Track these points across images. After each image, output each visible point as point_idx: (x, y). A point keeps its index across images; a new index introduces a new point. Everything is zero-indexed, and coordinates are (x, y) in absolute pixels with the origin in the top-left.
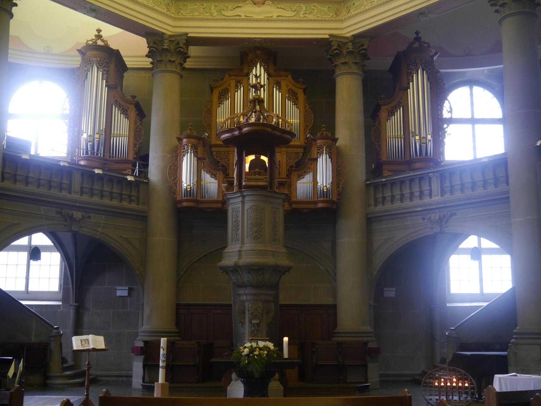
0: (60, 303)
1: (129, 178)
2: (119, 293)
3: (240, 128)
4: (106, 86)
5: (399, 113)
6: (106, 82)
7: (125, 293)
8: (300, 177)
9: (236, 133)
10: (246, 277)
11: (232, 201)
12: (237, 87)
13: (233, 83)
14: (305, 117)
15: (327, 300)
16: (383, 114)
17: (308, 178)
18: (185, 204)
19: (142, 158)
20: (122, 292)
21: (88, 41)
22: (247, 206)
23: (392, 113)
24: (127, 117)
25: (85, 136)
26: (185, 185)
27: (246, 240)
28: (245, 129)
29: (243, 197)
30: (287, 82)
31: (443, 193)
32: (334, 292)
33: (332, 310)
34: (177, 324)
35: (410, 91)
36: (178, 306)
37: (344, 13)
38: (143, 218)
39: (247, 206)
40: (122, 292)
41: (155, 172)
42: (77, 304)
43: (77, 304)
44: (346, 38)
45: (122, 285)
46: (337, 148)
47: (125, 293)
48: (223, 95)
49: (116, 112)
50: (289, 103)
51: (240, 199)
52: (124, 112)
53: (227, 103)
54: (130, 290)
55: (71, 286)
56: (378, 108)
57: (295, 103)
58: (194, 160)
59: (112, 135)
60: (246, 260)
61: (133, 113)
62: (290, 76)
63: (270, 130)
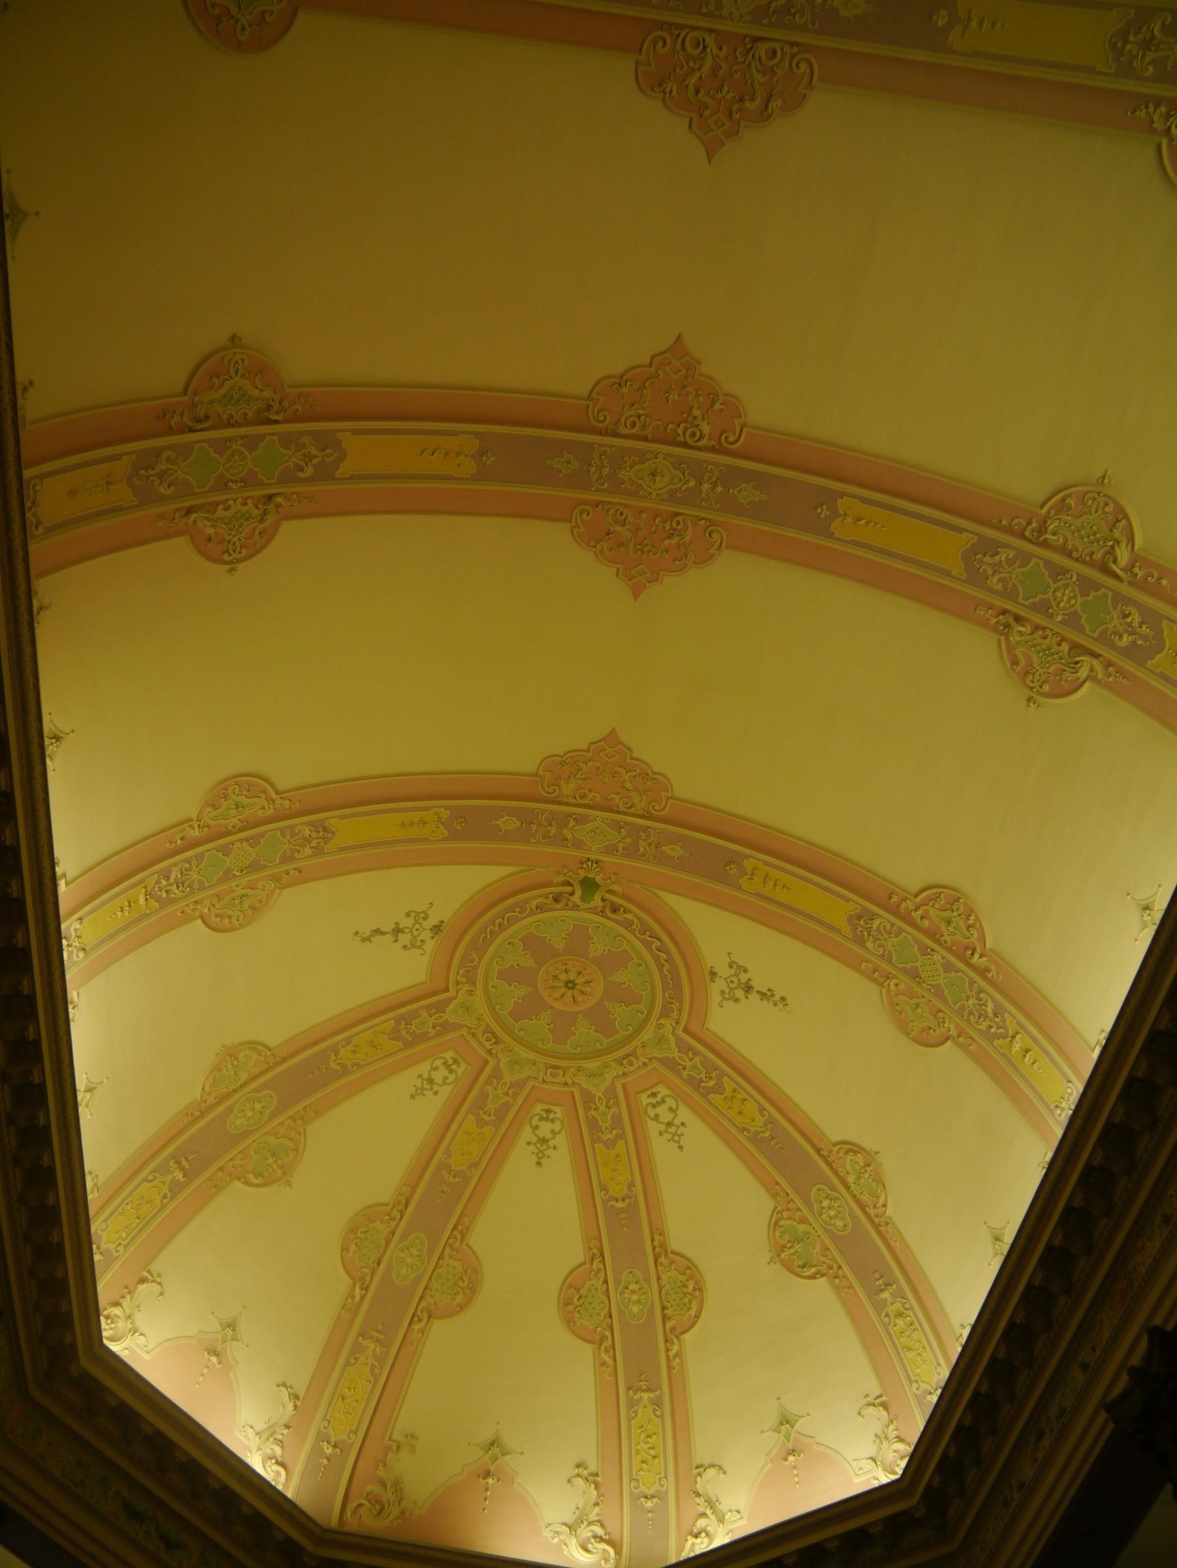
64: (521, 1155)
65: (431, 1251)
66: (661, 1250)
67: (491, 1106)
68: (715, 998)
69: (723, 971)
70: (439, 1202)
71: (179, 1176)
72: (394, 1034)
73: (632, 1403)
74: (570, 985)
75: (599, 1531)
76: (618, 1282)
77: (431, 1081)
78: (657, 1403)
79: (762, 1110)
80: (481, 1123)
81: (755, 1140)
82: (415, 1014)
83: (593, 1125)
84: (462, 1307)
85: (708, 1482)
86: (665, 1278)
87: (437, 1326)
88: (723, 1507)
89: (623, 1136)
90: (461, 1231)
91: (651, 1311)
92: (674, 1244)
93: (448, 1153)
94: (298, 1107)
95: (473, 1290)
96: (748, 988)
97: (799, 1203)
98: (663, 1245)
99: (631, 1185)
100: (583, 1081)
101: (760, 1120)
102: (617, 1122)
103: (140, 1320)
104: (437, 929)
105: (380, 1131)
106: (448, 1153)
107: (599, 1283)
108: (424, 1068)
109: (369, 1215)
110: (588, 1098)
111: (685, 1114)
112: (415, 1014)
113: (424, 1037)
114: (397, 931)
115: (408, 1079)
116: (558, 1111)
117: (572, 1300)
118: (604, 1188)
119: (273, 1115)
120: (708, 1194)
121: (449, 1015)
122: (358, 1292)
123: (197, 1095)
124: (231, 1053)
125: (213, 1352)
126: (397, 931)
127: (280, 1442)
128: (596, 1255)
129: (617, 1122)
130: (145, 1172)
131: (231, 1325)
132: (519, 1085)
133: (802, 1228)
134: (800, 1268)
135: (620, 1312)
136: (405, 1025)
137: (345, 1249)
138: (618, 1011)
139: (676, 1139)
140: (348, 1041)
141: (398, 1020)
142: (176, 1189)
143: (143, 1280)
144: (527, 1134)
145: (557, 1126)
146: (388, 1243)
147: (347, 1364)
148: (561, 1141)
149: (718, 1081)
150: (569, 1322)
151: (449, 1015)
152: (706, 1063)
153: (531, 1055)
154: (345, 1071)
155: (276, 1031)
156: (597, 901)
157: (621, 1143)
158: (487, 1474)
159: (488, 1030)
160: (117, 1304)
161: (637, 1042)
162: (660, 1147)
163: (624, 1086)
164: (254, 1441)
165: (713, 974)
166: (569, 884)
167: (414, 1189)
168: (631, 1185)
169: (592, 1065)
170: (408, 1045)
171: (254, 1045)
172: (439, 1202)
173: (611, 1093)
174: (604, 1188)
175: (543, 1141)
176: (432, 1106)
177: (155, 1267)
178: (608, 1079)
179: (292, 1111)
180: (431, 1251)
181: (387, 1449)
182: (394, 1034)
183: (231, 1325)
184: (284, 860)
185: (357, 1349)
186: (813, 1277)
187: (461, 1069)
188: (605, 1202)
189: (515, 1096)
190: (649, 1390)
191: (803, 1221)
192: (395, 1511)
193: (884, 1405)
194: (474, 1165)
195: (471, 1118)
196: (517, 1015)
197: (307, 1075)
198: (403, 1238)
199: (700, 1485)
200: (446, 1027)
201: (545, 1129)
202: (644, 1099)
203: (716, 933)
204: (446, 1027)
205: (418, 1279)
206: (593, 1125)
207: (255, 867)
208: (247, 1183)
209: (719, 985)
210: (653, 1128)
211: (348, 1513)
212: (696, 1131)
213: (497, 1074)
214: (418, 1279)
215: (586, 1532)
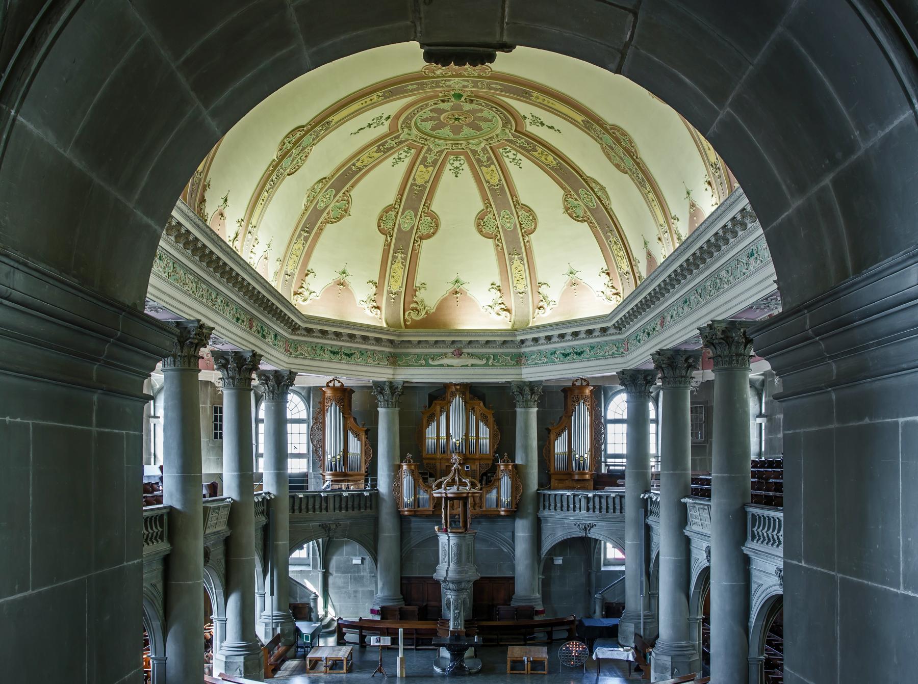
1: (366, 494)
2: (355, 562)
5: (565, 435)
7: (359, 562)
8: (488, 492)
10: (451, 586)
13: (438, 408)
14: (492, 437)
15: (508, 574)
16: (553, 436)
17: (492, 495)
18: (406, 513)
19: (372, 471)
20: (357, 561)
22: (452, 542)
23: (559, 435)
24: (359, 439)
25: (329, 456)
30: (480, 406)
31: (588, 510)
32: (513, 568)
33: (510, 581)
34: (402, 593)
35: (573, 418)
36: (402, 578)
37: (523, 361)
38: (376, 520)
39: (452, 542)
40: (357, 561)
41: (383, 485)
44: (525, 382)
45: (356, 555)
46: (516, 467)
48: (432, 418)
49: (351, 435)
50: (481, 424)
52: (357, 435)
53: (434, 424)
54: (363, 559)
55: (318, 557)
56: (549, 431)
57: (486, 424)
58: (412, 480)
60: (451, 575)
61: (363, 437)
62: (482, 404)
64: (447, 175)
65: (416, 216)
66: (517, 203)
67: (429, 160)
68: (528, 124)
69: (529, 116)
70: (416, 197)
71: (306, 234)
72: (378, 151)
73: (511, 260)
74: (456, 119)
75: (503, 306)
76: (499, 216)
77: (400, 159)
78: (522, 259)
79: (555, 159)
80: (425, 166)
81: (552, 168)
82: (386, 142)
83: (478, 161)
84: (434, 234)
85: (543, 290)
86: (520, 213)
87: (424, 242)
88: (550, 299)
89: (493, 163)
90: (427, 205)
91: (515, 225)
92: (522, 201)
93: (414, 179)
94: (345, 189)
95: (437, 226)
96: (542, 124)
97: (573, 193)
98: (517, 201)
99: (500, 180)
100: (470, 147)
101: (555, 163)
102: (489, 159)
103: (312, 289)
104: (388, 118)
105: (383, 183)
106: (414, 179)
107: (491, 216)
108: (396, 156)
109: (387, 210)
110: (474, 152)
111: (519, 156)
112: (386, 142)
113: (392, 148)
114: (369, 125)
115: (390, 160)
116: (462, 157)
117: (480, 223)
118: (488, 182)
119: (335, 196)
120: (533, 184)
121: (402, 137)
122: (389, 239)
123: (303, 207)
124: (313, 189)
125: (342, 284)
126: (369, 125)
127: (374, 301)
128: (488, 205)
129: (489, 159)
130: (294, 241)
131: (344, 272)
132: (442, 151)
133: (576, 202)
134: (576, 218)
135: (502, 226)
136: (382, 147)
137: (379, 226)
138: (482, 124)
139: (518, 164)
140: (358, 160)
141: (378, 147)
142: (306, 239)
143: (307, 275)
144: (448, 166)
145: (462, 162)
146: (396, 217)
147: (392, 264)
148: (466, 166)
149: (533, 147)
150: (480, 232)
151: (402, 137)
152: (526, 141)
153: (444, 142)
154: (360, 169)
155: (326, 173)
156: (463, 99)
157: (493, 167)
158: (457, 293)
159: (421, 138)
160: (302, 287)
161: (494, 134)
162: (512, 168)
163: (491, 148)
164: (365, 305)
165: (525, 118)
166: (445, 96)
167: (402, 195)
168: (500, 180)
169: (474, 141)
170: (385, 153)
171: (321, 181)
172: (416, 197)
173: (484, 149)
174: (488, 182)
175: (457, 168)
176: (403, 167)
177: (309, 268)
178: (482, 145)
179: (343, 191)
180: (416, 216)
181: (416, 290)
182: (378, 151)
183: (344, 272)
184: (314, 140)
185: (394, 258)
186: (581, 221)
187: (413, 151)
188: (489, 187)
189: (440, 156)
190: (518, 254)
191: (576, 200)
192: (424, 312)
193: (608, 274)
194: (428, 182)
195: (422, 167)
196: (433, 129)
197: (346, 177)
198: (403, 214)
199: (540, 290)
200: (401, 142)
201: (457, 164)
202: (501, 150)
203: (522, 107)
204: (401, 142)
205: (412, 227)
206: (478, 161)
207: (304, 148)
208: (332, 222)
209: (527, 121)
210: (507, 160)
211: (406, 316)
212: (526, 162)
213: (429, 150)
214: (412, 227)
215: (497, 308)
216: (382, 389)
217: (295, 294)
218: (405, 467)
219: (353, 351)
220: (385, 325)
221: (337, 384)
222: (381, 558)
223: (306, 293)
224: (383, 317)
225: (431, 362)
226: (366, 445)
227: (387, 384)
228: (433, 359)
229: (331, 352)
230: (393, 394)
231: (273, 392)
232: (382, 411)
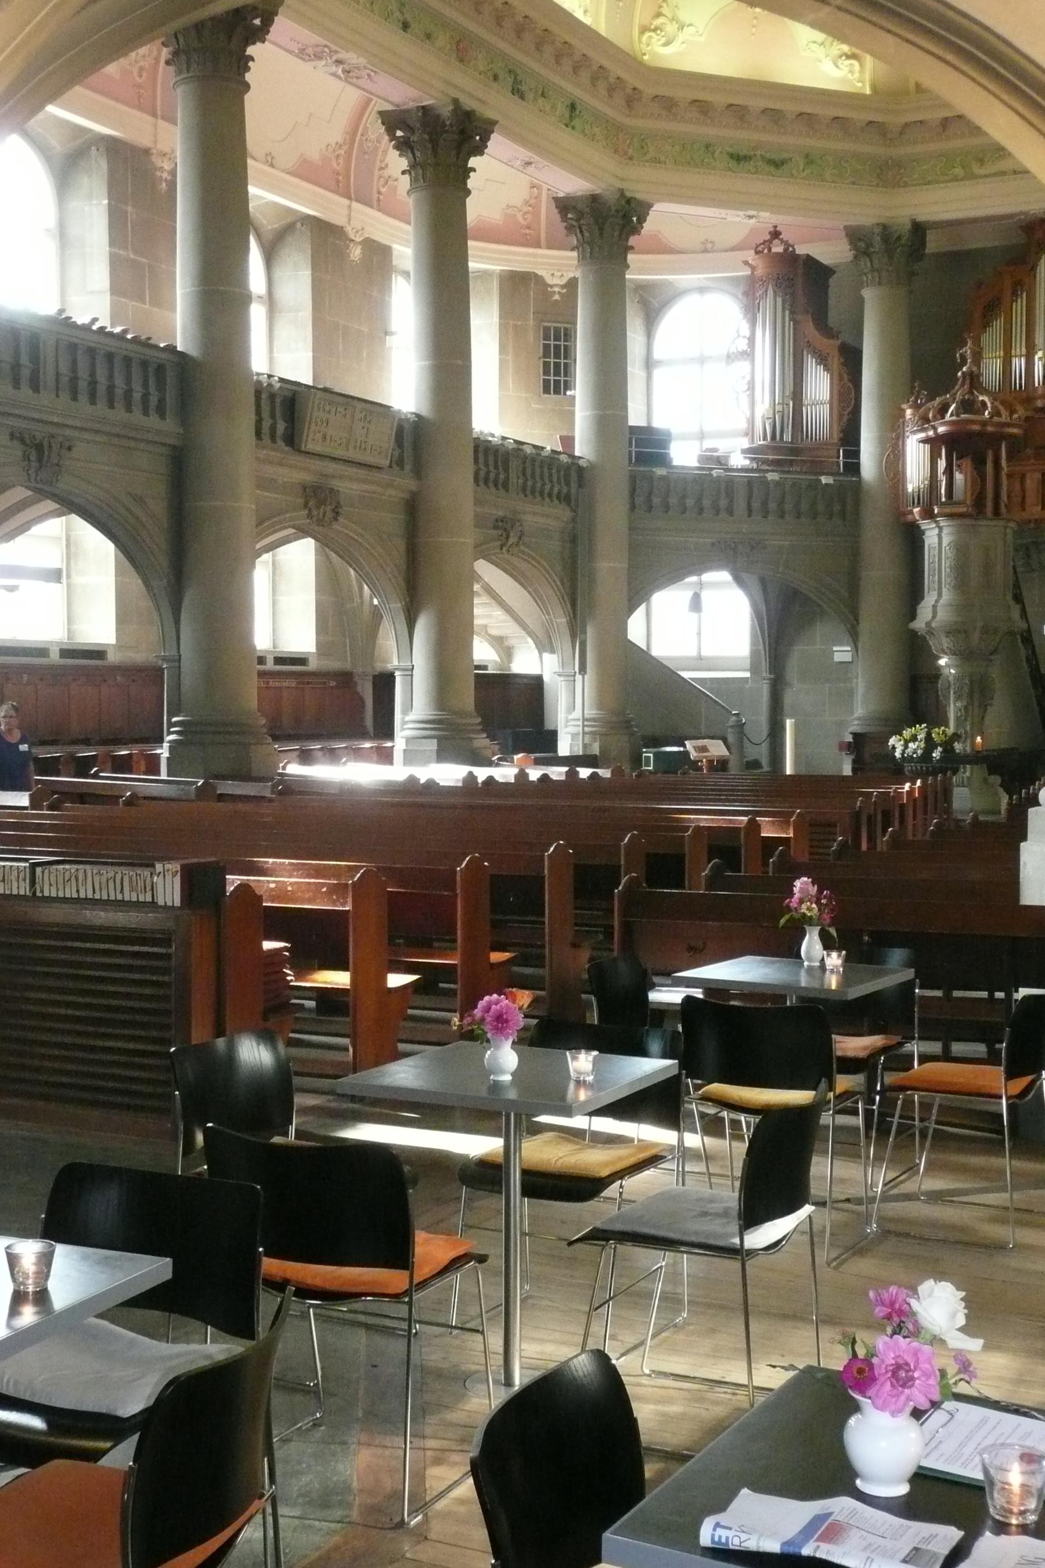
0: (747, 675)
2: (838, 657)
3: (935, 428)
4: (790, 320)
6: (792, 313)
9: (931, 433)
11: (928, 533)
12: (1015, 294)
21: (757, 246)
24: (827, 368)
26: (910, 488)
27: (944, 591)
28: (941, 430)
29: (940, 529)
42: (772, 676)
43: (772, 676)
45: (841, 644)
47: (848, 657)
51: (936, 531)
52: (823, 360)
53: (998, 324)
59: (805, 402)
61: (836, 361)
63: (976, 428)
164: (820, 52)
216: (870, 245)
217: (644, 30)
218: (909, 412)
219: (786, 155)
220: (868, 91)
221: (777, 248)
222: (864, 627)
223: (671, 28)
224: (867, 77)
225: (977, 170)
226: (841, 379)
227: (877, 230)
228: (981, 162)
229: (731, 156)
230: (889, 252)
231: (591, 243)
232: (867, 293)
